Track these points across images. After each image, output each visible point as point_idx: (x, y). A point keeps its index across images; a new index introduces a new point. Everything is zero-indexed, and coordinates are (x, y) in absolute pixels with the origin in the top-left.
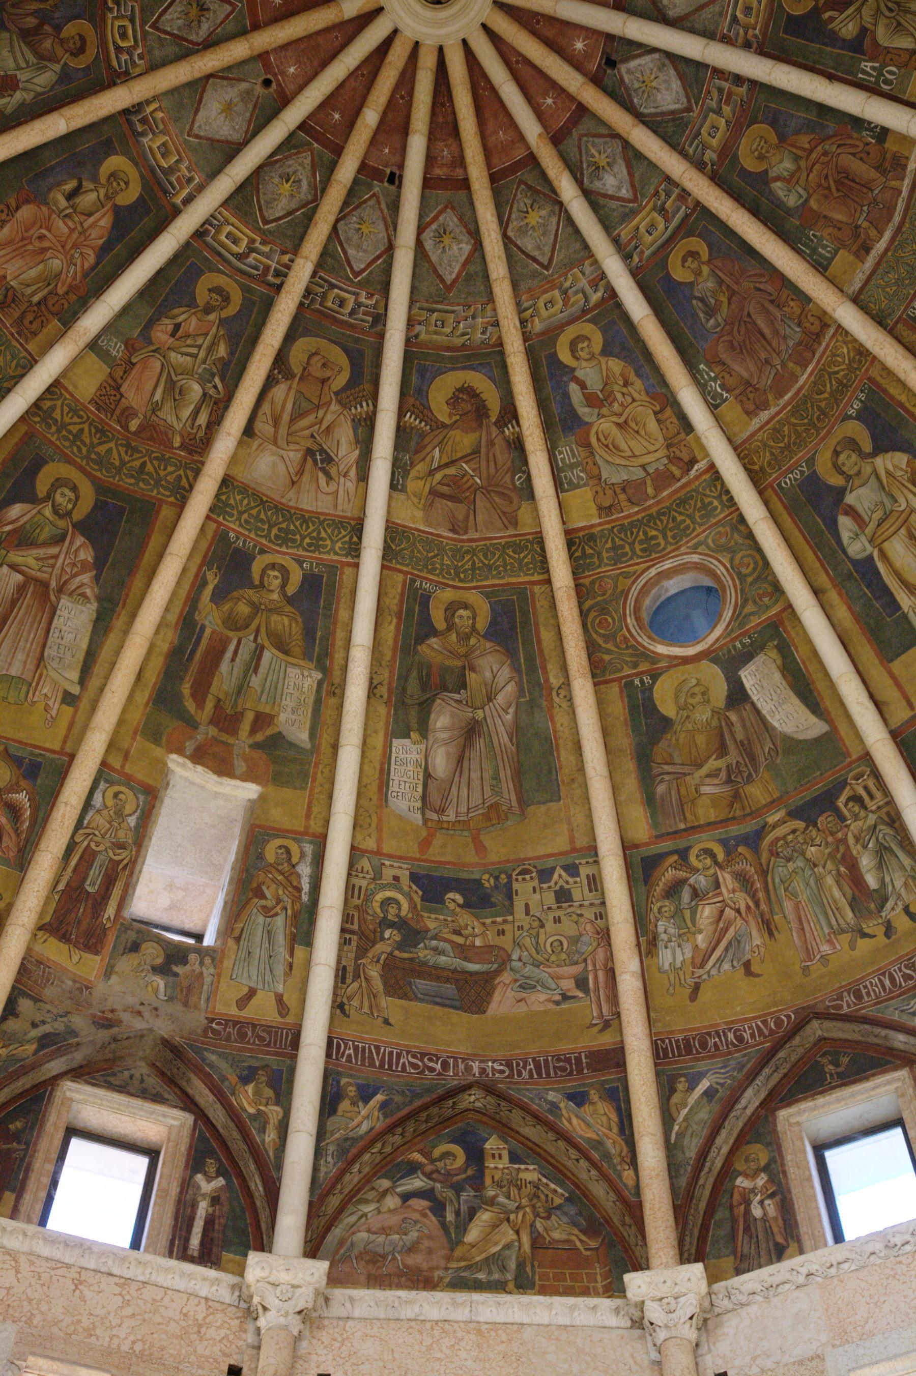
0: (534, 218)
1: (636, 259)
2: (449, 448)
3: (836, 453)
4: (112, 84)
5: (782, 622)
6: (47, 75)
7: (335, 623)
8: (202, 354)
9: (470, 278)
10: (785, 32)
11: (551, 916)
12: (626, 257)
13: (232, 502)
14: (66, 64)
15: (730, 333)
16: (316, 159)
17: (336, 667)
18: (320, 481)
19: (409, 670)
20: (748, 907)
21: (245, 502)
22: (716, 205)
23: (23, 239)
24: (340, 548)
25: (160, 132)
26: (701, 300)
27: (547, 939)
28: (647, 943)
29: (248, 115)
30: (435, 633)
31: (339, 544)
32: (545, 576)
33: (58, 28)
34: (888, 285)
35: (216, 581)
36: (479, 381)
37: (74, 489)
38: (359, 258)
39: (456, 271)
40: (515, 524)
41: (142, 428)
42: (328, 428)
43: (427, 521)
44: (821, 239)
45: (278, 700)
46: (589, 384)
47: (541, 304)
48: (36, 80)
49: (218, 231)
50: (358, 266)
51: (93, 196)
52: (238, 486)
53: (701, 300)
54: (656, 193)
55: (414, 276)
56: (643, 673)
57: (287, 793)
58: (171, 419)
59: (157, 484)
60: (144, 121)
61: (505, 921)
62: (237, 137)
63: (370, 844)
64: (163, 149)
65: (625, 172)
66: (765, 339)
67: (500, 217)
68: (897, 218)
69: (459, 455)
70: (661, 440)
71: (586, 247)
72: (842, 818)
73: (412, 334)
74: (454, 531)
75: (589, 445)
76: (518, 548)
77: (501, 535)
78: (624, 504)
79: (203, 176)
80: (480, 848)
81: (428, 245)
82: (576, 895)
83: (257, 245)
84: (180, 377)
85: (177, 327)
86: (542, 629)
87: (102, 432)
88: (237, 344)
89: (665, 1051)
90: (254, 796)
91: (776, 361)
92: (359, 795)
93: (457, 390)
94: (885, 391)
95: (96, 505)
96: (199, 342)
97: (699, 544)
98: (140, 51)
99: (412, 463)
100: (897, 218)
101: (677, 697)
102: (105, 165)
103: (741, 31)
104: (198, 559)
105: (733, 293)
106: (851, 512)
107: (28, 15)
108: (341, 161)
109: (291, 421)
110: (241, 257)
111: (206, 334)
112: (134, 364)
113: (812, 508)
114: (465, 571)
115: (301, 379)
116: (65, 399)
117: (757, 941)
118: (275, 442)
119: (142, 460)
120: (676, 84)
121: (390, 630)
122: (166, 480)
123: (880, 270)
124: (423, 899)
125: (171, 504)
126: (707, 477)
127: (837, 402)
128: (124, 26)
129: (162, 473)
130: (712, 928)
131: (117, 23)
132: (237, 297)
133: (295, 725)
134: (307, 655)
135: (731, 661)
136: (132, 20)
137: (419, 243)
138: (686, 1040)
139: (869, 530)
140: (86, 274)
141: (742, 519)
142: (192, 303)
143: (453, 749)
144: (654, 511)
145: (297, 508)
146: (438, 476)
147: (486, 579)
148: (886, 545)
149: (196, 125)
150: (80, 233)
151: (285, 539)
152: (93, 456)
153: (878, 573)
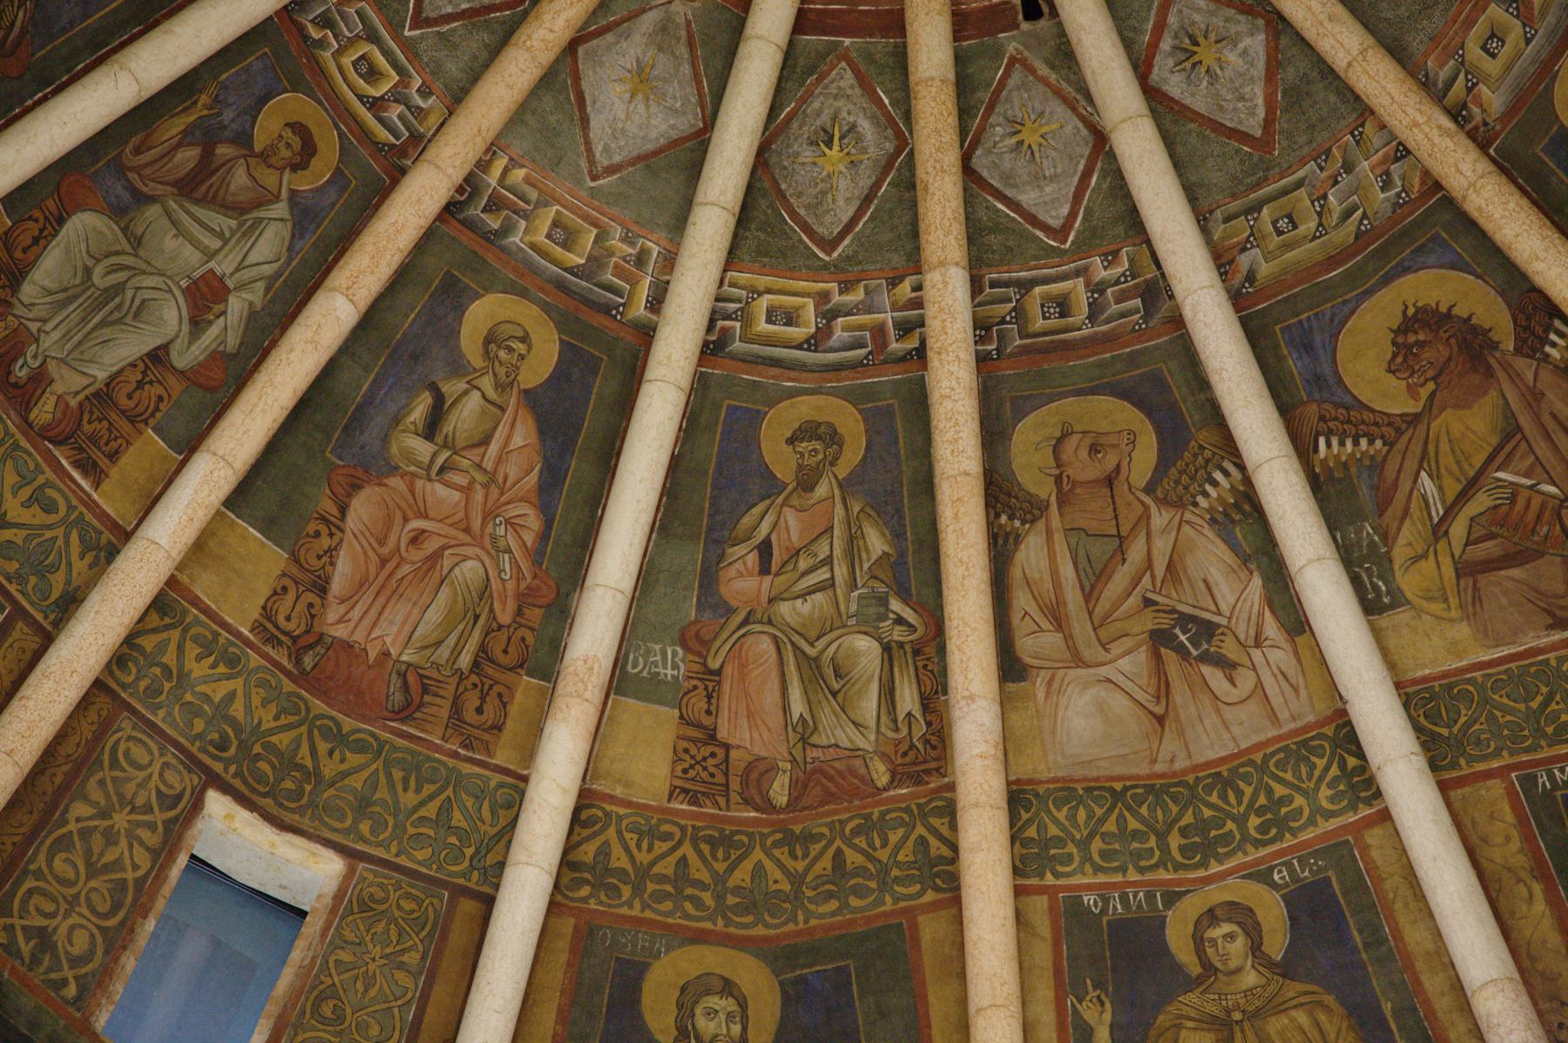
2: (1447, 460)
4: (398, 175)
6: (269, 234)
7: (1409, 965)
8: (841, 572)
9: (1296, 97)
13: (1053, 830)
14: (293, 194)
16: (863, 67)
18: (1213, 683)
21: (1082, 815)
23: (384, 562)
24: (1331, 799)
25: (538, 205)
29: (686, 69)
31: (1325, 792)
33: (244, 139)
35: (1108, 1016)
36: (1431, 286)
37: (727, 987)
38: (1050, 200)
39: (1260, 101)
41: (799, 787)
42: (1170, 567)
43: (1488, 636)
47: (1474, 51)
48: (252, 259)
49: (745, 316)
50: (1055, 217)
51: (474, 399)
52: (1049, 792)
55: (1178, 164)
58: (846, 736)
59: (884, 886)
60: (495, 204)
62: (689, 122)
64: (559, 234)
69: (1478, 461)
73: (1237, 280)
79: (663, 235)
81: (1175, 86)
83: (837, 298)
84: (820, 644)
85: (765, 549)
87: (724, 841)
88: (899, 512)
93: (1397, 332)
95: (786, 999)
96: (823, 551)
98: (417, 82)
99: (1385, 536)
102: (466, 330)
104: (1045, 991)
107: (175, 149)
108: (910, 39)
109: (1087, 598)
110: (814, 343)
111: (830, 529)
112: (719, 672)
115: (1062, 503)
116: (620, 818)
118: (1078, 661)
119: (831, 851)
122: (897, 864)
125: (933, 907)
128: (362, 57)
129: (883, 855)
131: (347, 61)
132: (850, 423)
136: (373, 38)
137: (1153, 95)
140: (537, 556)
142: (771, 487)
145: (1196, 768)
146: (1458, 530)
149: (598, 149)
150: (486, 486)
151: (1204, 845)
152: (731, 900)
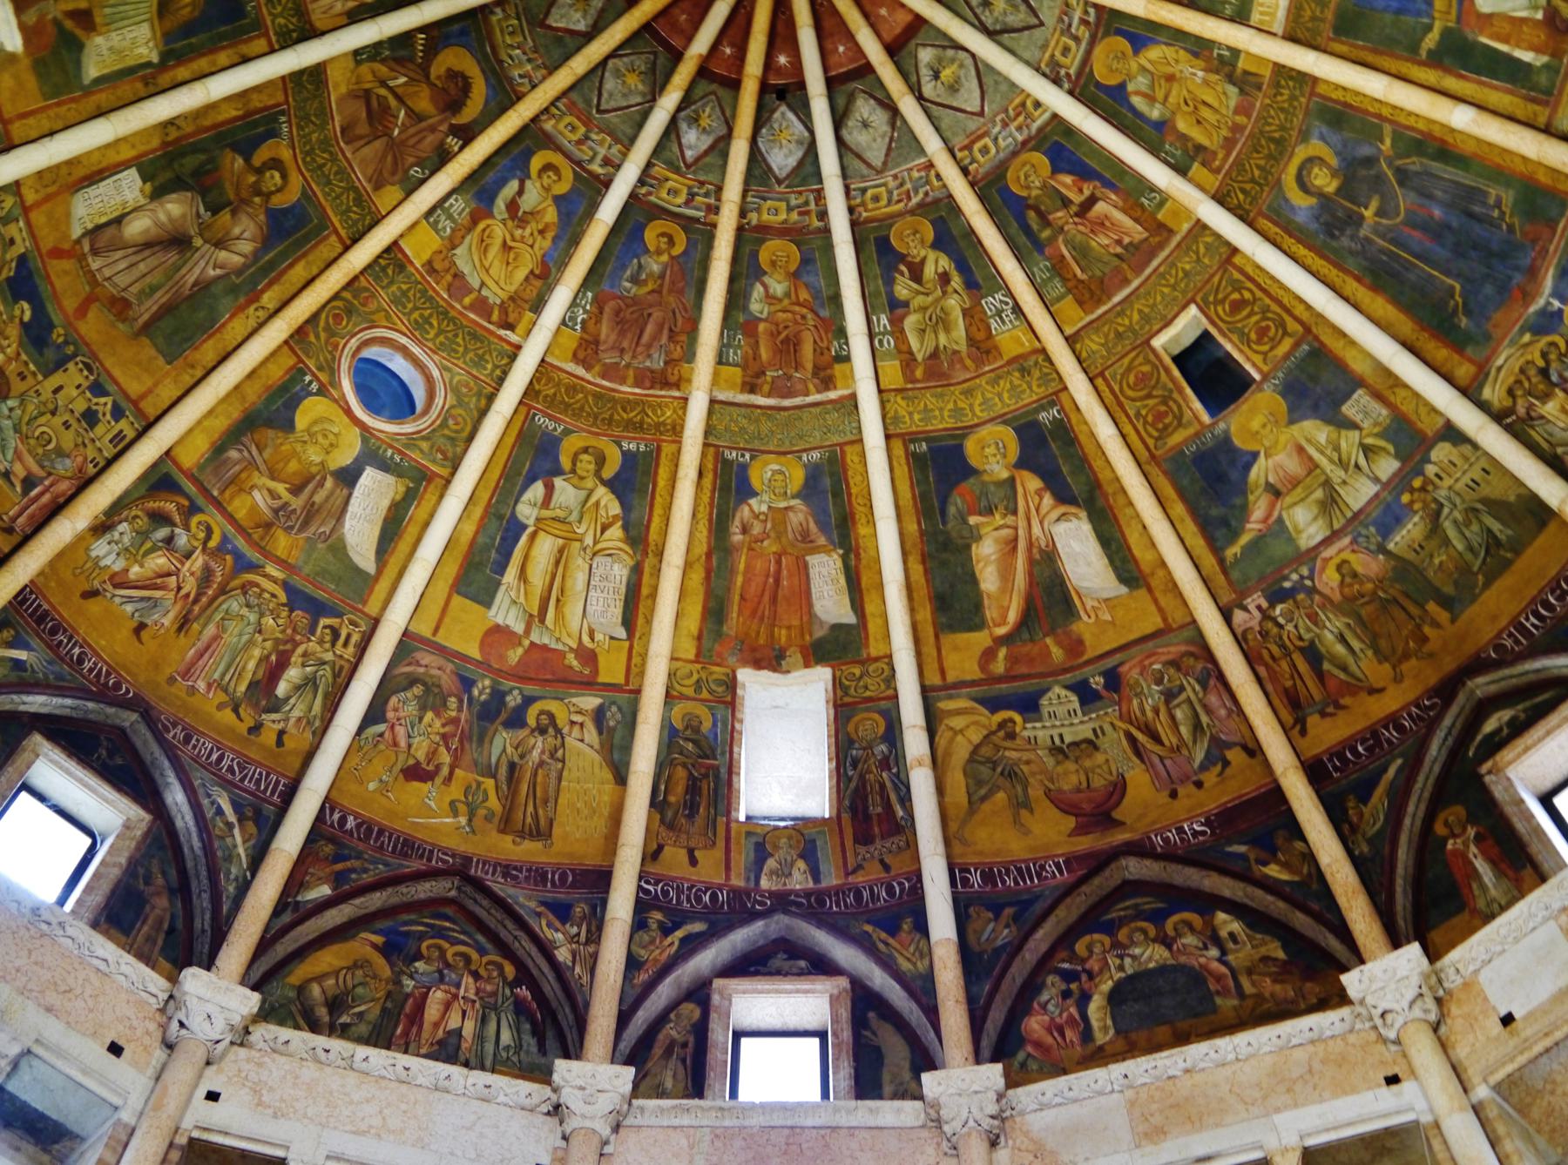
0: (633, 81)
1: (644, 190)
3: (585, 450)
5: (429, 481)
10: (876, 239)
11: (67, 417)
12: (641, 181)
15: (628, 306)
17: (171, 74)
19: (204, 151)
20: (187, 595)
22: (723, 243)
26: (640, 266)
27: (46, 425)
28: (102, 527)
30: (247, 160)
32: (349, 242)
34: (736, 422)
40: (378, 187)
43: (341, 100)
44: (739, 346)
45: (113, 26)
46: (525, 197)
47: (568, 119)
53: (640, 266)
54: (702, 183)
56: (318, 380)
57: (31, 82)
61: (34, 374)
63: (30, 197)
65: (704, 147)
66: (640, 337)
67: (621, 46)
68: (787, 403)
69: (409, 103)
70: (512, 288)
71: (633, 140)
72: (312, 631)
74: (343, 131)
75: (474, 221)
76: (359, 201)
77: (361, 177)
78: (444, 282)
80: (82, 311)
82: (100, 429)
86: (302, 264)
89: (25, 600)
90: (9, 47)
91: (627, 358)
92: (69, 163)
94: (657, 465)
97: (448, 369)
100: (787, 403)
101: (315, 422)
103: (858, 201)
105: (658, 291)
106: (550, 489)
113: (534, 456)
114: (314, 160)
117: (167, 621)
120: (792, 162)
121: (231, 112)
123: (743, 410)
124: (8, 279)
126: (507, 347)
127: (626, 428)
130: (150, 574)
133: (100, 55)
134: (168, 37)
135: (372, 455)
138: (46, 613)
139: (546, 513)
141: (491, 398)
143: (154, 231)
144: (453, 313)
146: (383, 92)
147: (318, 184)
148: (542, 534)
153: (517, 541)
